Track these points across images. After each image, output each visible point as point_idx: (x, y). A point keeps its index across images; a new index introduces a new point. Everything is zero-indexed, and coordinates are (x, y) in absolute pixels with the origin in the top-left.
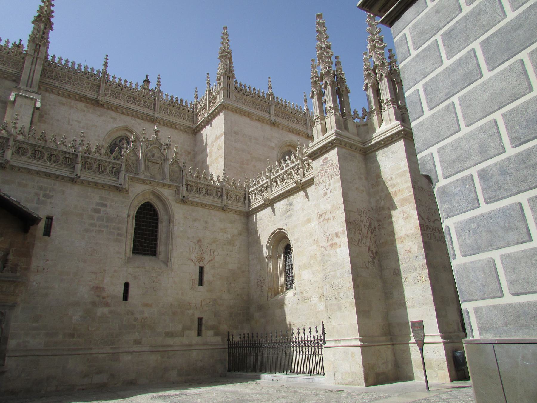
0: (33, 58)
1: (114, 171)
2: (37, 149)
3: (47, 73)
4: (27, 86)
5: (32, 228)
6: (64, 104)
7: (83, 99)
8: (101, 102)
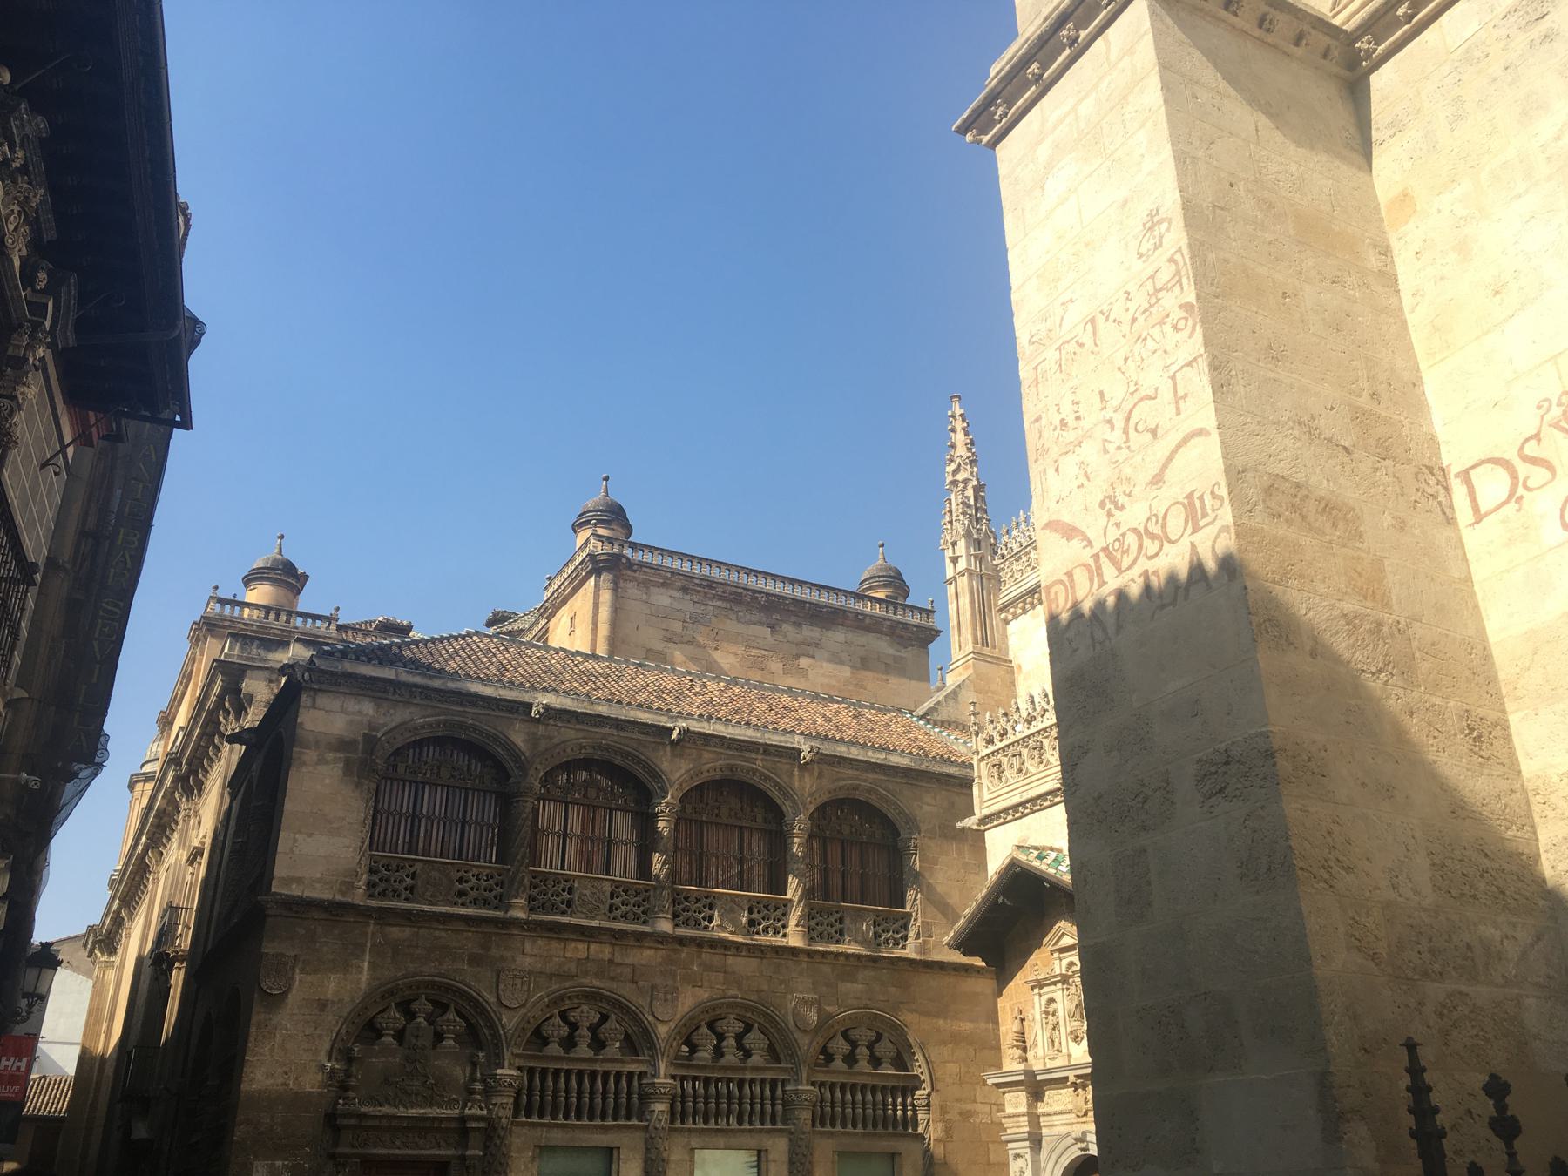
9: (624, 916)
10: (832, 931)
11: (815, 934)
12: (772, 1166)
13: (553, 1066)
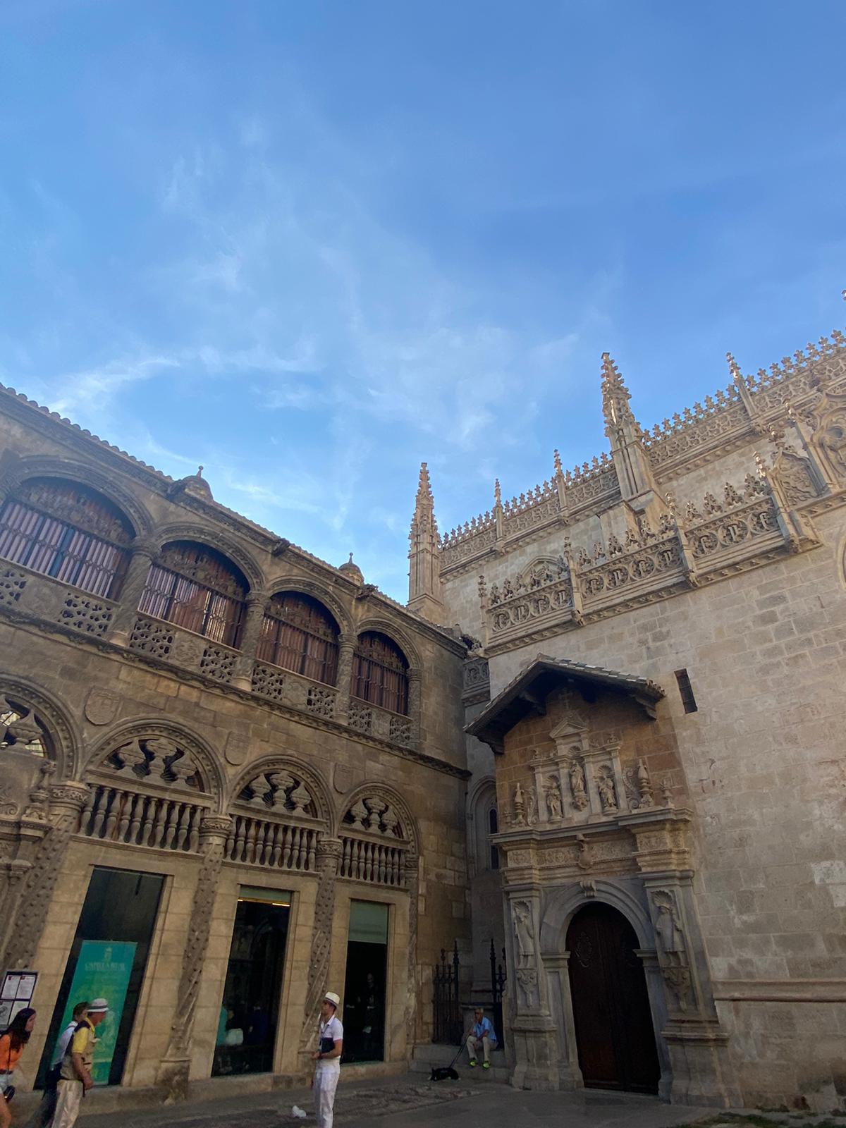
1: (763, 521)
2: (612, 567)
4: (632, 494)
5: (658, 705)
6: (705, 479)
7: (728, 448)
8: (758, 429)
9: (213, 672)
10: (364, 721)
11: (352, 721)
12: (302, 908)
13: (124, 787)
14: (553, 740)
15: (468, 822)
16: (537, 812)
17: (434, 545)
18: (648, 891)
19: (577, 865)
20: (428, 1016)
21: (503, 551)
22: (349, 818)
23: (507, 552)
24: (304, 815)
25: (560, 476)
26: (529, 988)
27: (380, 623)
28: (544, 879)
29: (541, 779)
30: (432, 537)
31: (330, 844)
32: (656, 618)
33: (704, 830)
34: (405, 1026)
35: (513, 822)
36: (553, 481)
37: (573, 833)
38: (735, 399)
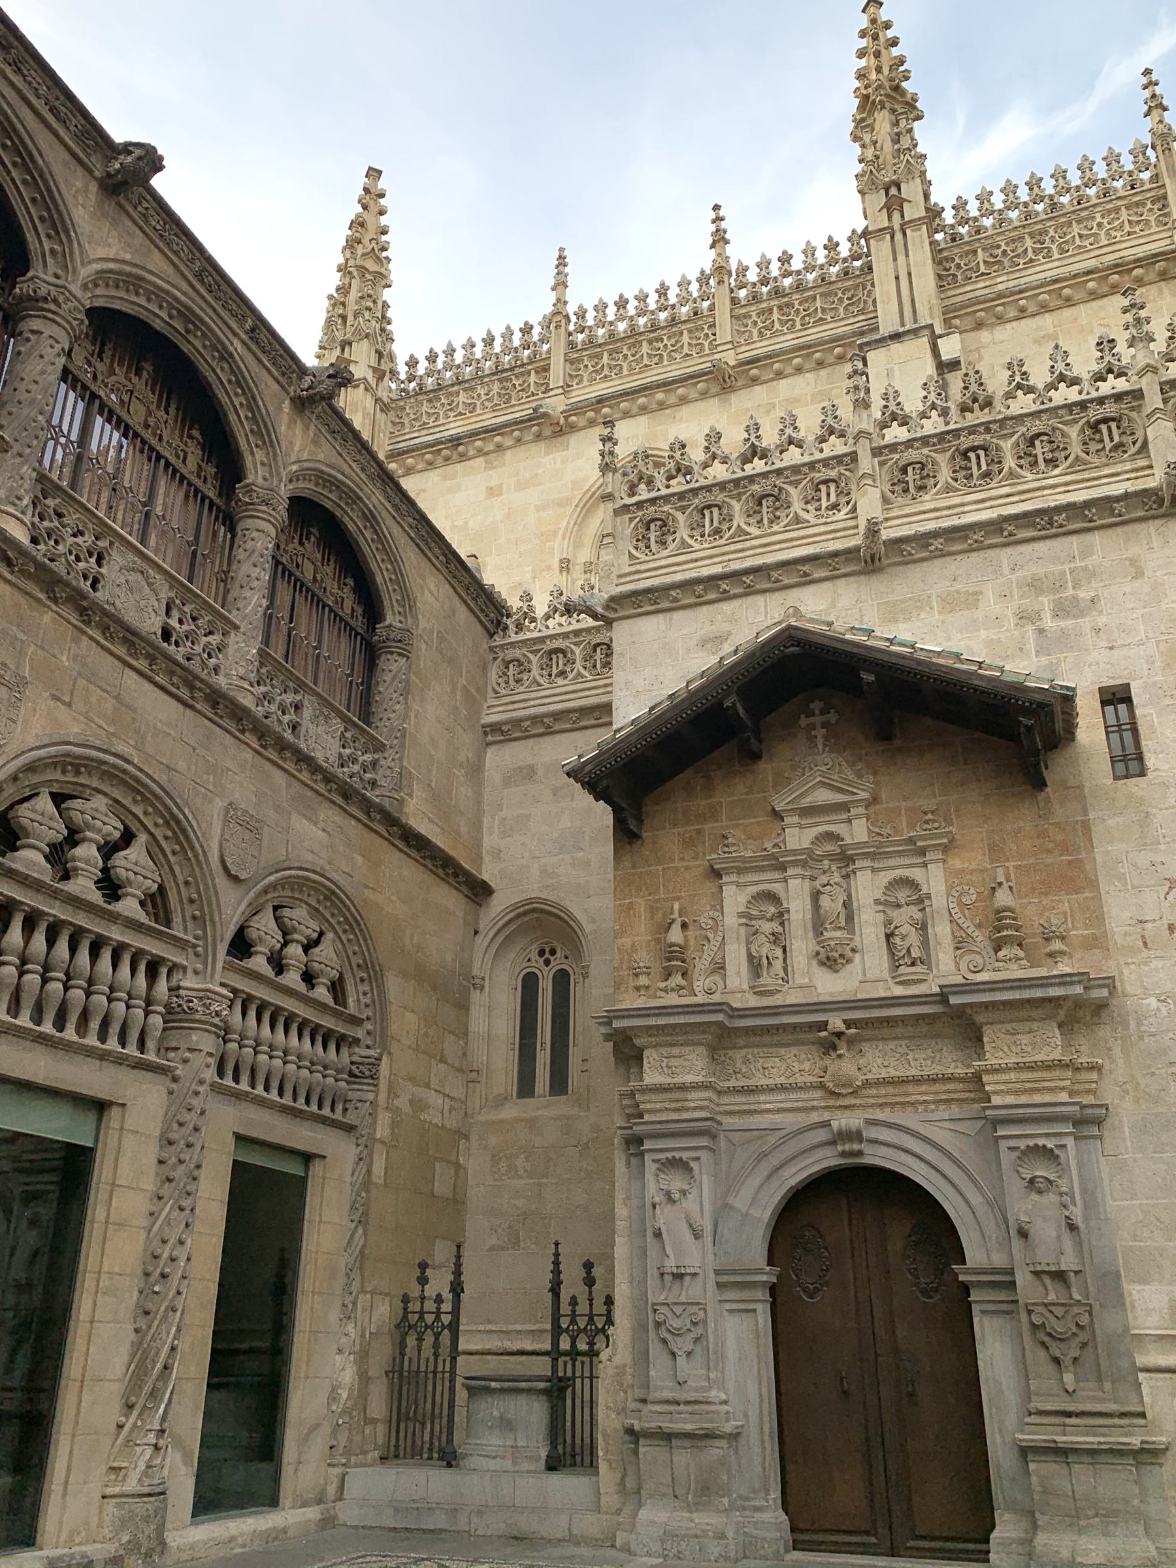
0: (892, 238)
2: (966, 442)
3: (958, 266)
14: (777, 816)
15: (475, 996)
16: (719, 968)
17: (380, 378)
18: (1003, 1145)
19: (822, 1086)
20: (378, 1406)
21: (562, 421)
22: (241, 946)
23: (573, 428)
24: (141, 916)
25: (721, 270)
26: (682, 1345)
27: (337, 485)
28: (731, 1113)
29: (735, 898)
30: (380, 354)
31: (205, 996)
32: (1066, 567)
33: (1139, 1025)
34: (326, 1429)
35: (662, 985)
36: (703, 279)
37: (821, 1017)
38: (1146, 176)
